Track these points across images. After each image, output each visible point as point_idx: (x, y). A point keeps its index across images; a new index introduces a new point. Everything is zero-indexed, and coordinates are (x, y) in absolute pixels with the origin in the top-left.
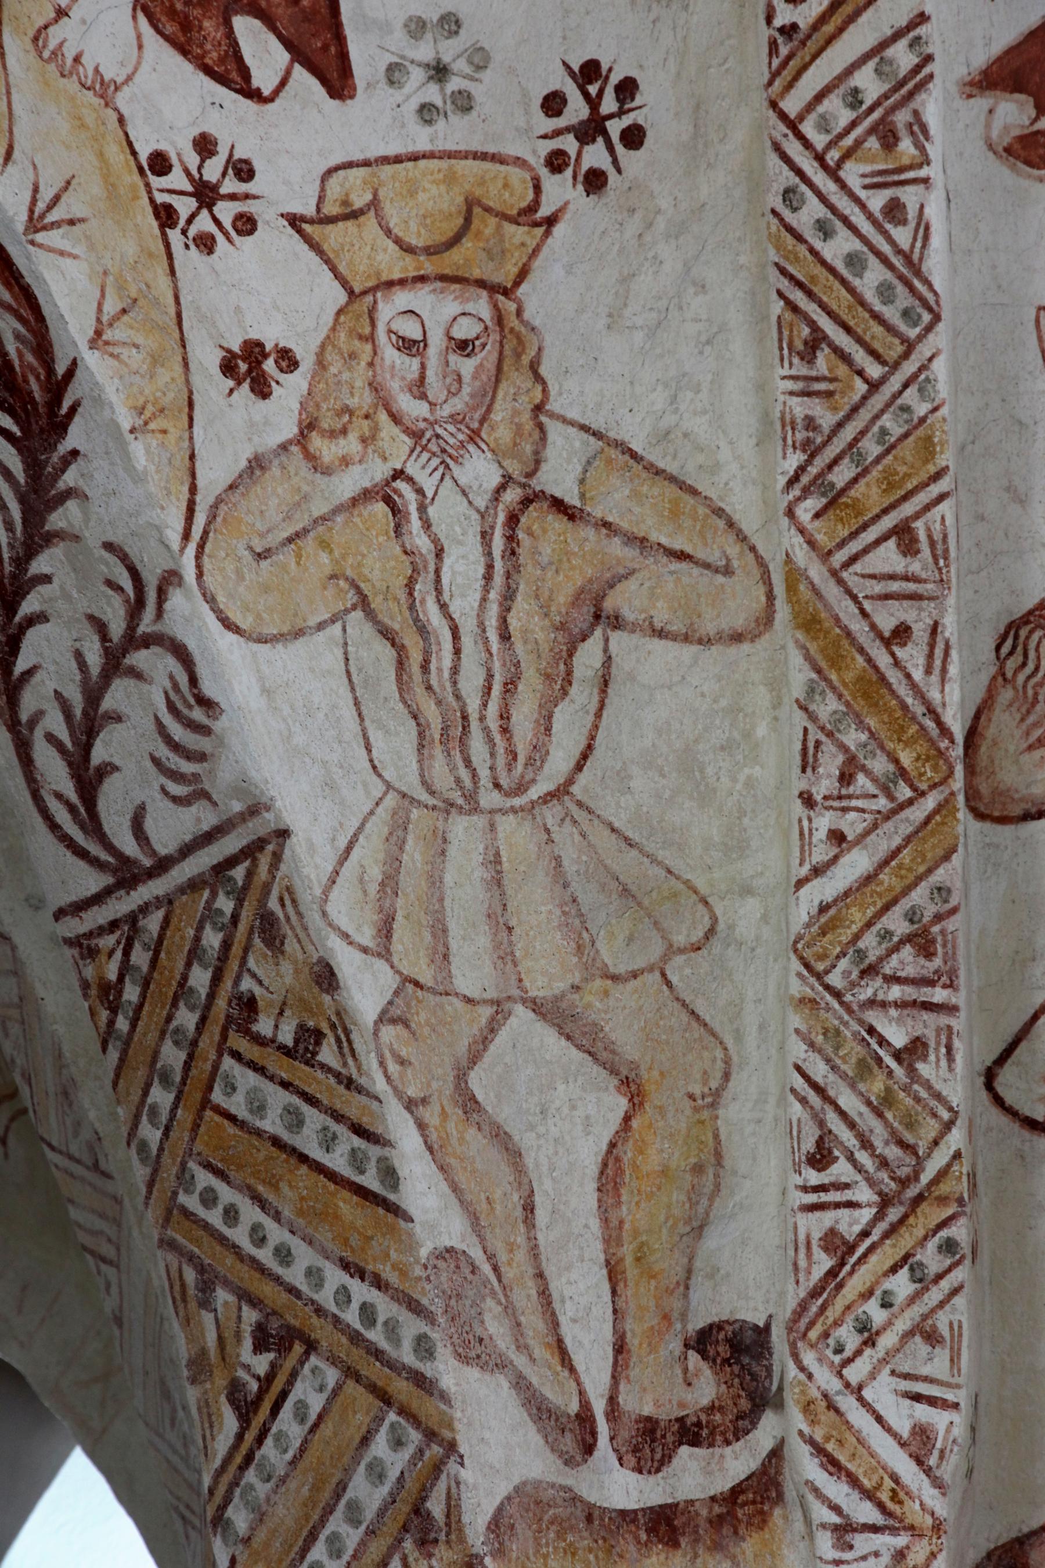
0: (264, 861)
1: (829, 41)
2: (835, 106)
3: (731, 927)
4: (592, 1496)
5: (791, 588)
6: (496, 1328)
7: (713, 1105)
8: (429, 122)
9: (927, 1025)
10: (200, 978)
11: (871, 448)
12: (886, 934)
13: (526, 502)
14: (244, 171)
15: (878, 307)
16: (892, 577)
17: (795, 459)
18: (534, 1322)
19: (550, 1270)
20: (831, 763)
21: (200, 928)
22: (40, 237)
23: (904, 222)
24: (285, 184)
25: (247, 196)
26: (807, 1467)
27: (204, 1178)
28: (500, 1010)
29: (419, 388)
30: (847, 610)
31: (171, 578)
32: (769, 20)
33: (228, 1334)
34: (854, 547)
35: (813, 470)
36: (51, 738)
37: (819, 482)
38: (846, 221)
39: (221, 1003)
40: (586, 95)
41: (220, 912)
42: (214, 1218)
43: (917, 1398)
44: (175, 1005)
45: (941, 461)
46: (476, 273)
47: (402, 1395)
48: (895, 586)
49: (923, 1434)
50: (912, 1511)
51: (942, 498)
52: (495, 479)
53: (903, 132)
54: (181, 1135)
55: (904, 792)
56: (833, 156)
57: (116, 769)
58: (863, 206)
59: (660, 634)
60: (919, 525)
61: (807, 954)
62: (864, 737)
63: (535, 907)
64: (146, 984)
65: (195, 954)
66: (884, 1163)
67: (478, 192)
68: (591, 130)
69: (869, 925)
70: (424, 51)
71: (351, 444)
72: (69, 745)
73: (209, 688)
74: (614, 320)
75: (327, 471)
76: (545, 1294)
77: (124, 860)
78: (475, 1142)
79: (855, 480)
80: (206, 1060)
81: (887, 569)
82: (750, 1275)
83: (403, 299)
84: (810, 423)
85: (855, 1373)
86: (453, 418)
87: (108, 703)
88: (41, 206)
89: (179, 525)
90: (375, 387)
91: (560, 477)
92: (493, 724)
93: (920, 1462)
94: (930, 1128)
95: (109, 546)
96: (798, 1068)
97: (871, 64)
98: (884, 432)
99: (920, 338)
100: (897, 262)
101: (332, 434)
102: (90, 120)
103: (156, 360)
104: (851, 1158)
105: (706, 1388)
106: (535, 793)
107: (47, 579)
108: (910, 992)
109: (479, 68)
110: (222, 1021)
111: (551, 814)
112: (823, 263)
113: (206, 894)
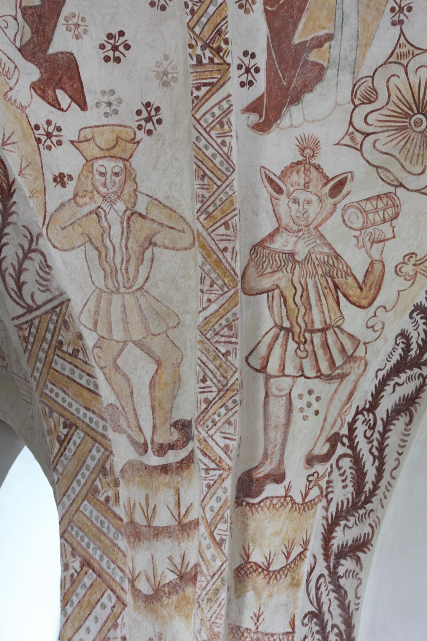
0: (64, 307)
1: (207, 100)
2: (208, 116)
3: (184, 322)
4: (147, 463)
5: (198, 238)
6: (123, 423)
7: (179, 367)
8: (107, 117)
9: (230, 347)
10: (49, 336)
11: (218, 202)
12: (221, 325)
13: (132, 214)
14: (59, 129)
15: (220, 167)
16: (223, 235)
17: (199, 205)
18: (133, 421)
19: (137, 408)
20: (208, 282)
21: (48, 323)
22: (5, 147)
23: (226, 146)
24: (69, 133)
25: (60, 136)
26: (199, 455)
27: (50, 386)
28: (125, 343)
29: (105, 185)
30: (212, 243)
31: (40, 235)
32: (192, 94)
33: (57, 424)
34: (214, 227)
35: (204, 208)
36: (10, 274)
37: (205, 211)
38: (211, 145)
39: (54, 342)
40: (147, 111)
41: (53, 320)
42: (53, 395)
43: (226, 438)
44: (42, 342)
45: (235, 206)
46: (119, 156)
47: (99, 439)
48: (224, 238)
49: (227, 447)
50: (224, 465)
51: (235, 215)
52: (124, 208)
53: (225, 124)
54: (44, 375)
55: (226, 289)
56: (208, 129)
57: (26, 283)
58: (216, 142)
59: (166, 248)
60: (230, 222)
61: (201, 330)
62: (216, 275)
63: (134, 318)
64: (35, 337)
66: (219, 381)
67: (120, 135)
68: (149, 119)
69: (217, 322)
70: (106, 99)
71: (87, 199)
73: (49, 263)
74: (155, 168)
75: (81, 206)
76: (135, 414)
77: (29, 306)
78: (118, 377)
79: (214, 211)
81: (222, 233)
82: (187, 407)
83: (100, 162)
84: (203, 196)
85: (211, 433)
86: (114, 193)
87: (24, 266)
88: (5, 139)
89: (42, 221)
90: (93, 185)
91: (141, 208)
92: (124, 271)
93: (226, 453)
94: (231, 373)
95: (24, 226)
96: (199, 358)
97: (217, 106)
98: (221, 198)
99: (230, 175)
100: (224, 156)
101: (82, 197)
102: (19, 116)
103: (36, 178)
104: (211, 380)
105: (176, 436)
106: (134, 288)
107: (8, 234)
108: (226, 339)
109: (120, 103)
111: (138, 294)
112: (206, 156)
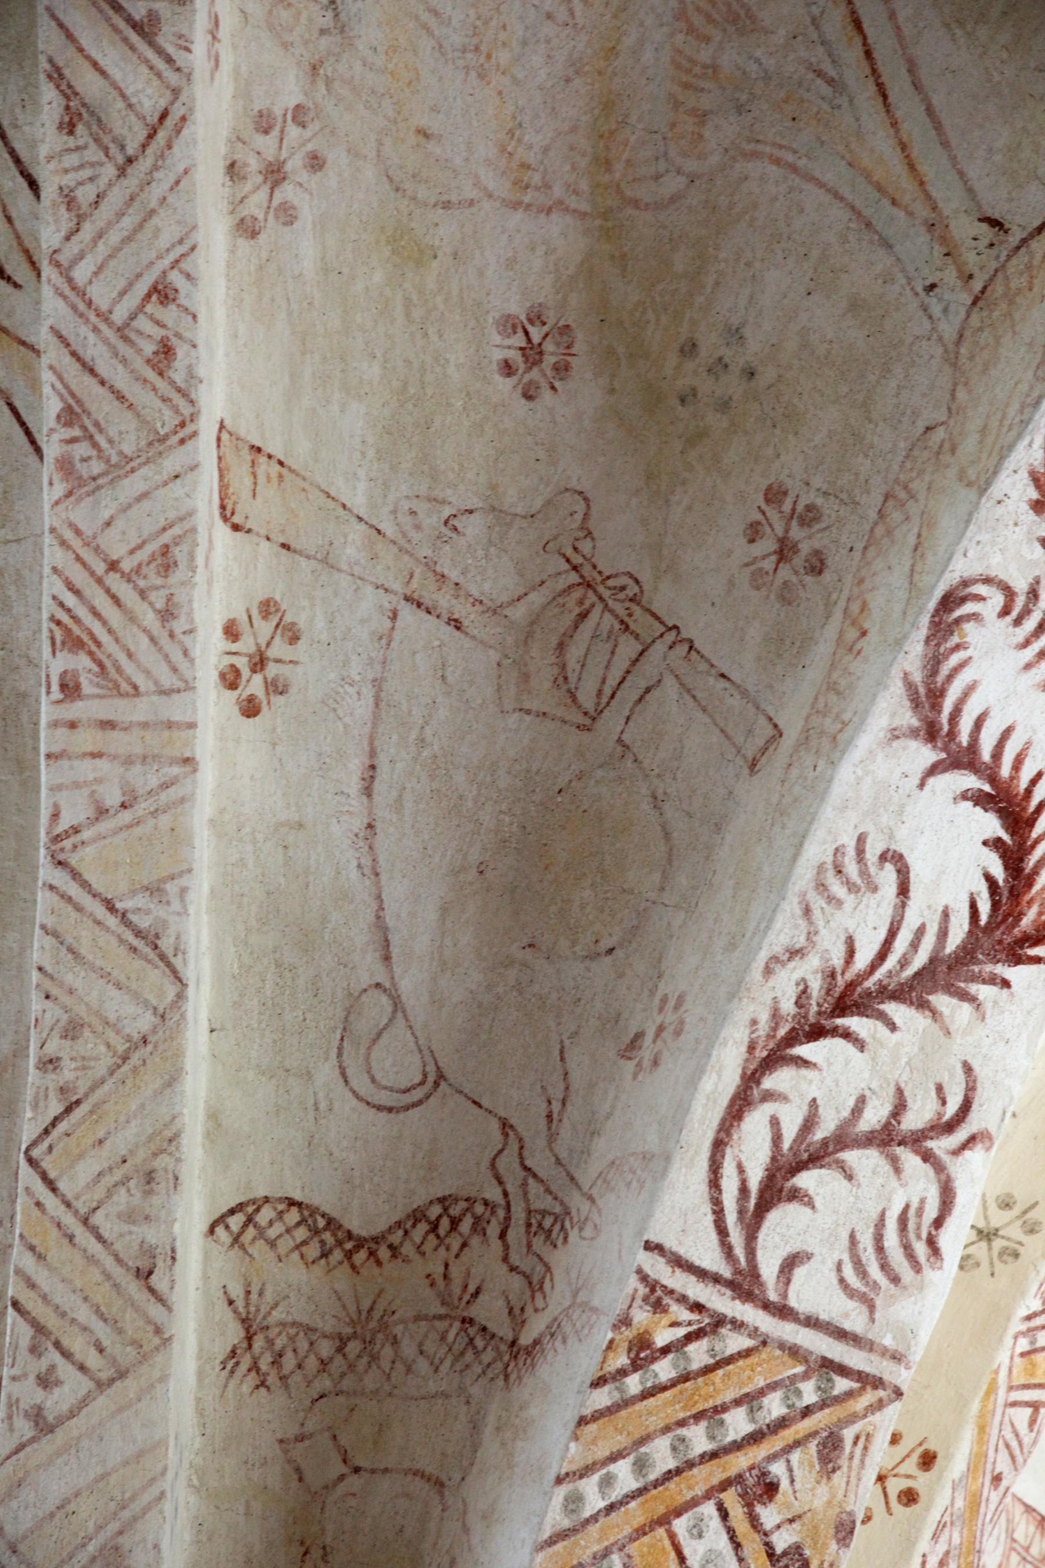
0: (869, 1397)
10: (738, 1424)
21: (773, 1387)
36: (775, 1122)
39: (740, 1462)
41: (799, 1393)
44: (698, 1417)
57: (811, 1204)
64: (685, 1378)
65: (750, 1400)
72: (786, 1145)
77: (754, 1274)
80: (690, 1488)
95: (968, 1069)
107: (893, 1027)
110: (732, 1472)
113: (800, 1369)
